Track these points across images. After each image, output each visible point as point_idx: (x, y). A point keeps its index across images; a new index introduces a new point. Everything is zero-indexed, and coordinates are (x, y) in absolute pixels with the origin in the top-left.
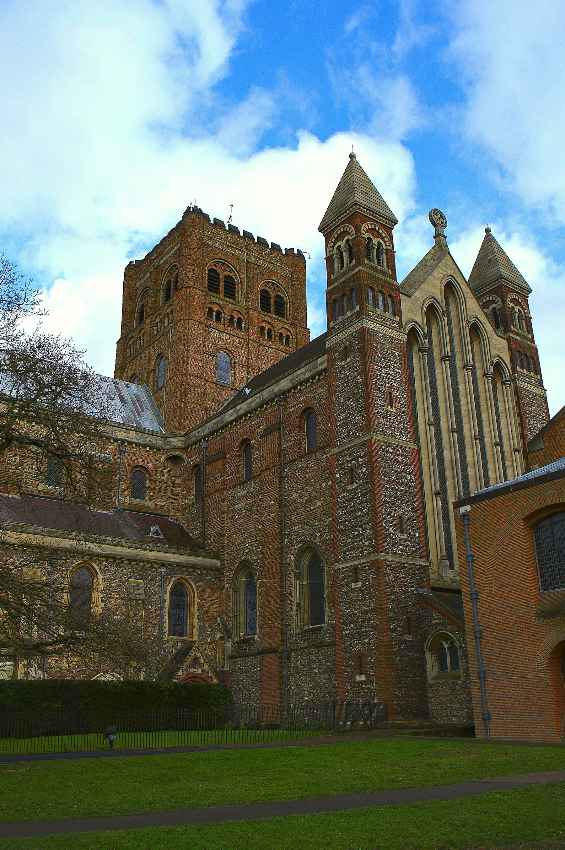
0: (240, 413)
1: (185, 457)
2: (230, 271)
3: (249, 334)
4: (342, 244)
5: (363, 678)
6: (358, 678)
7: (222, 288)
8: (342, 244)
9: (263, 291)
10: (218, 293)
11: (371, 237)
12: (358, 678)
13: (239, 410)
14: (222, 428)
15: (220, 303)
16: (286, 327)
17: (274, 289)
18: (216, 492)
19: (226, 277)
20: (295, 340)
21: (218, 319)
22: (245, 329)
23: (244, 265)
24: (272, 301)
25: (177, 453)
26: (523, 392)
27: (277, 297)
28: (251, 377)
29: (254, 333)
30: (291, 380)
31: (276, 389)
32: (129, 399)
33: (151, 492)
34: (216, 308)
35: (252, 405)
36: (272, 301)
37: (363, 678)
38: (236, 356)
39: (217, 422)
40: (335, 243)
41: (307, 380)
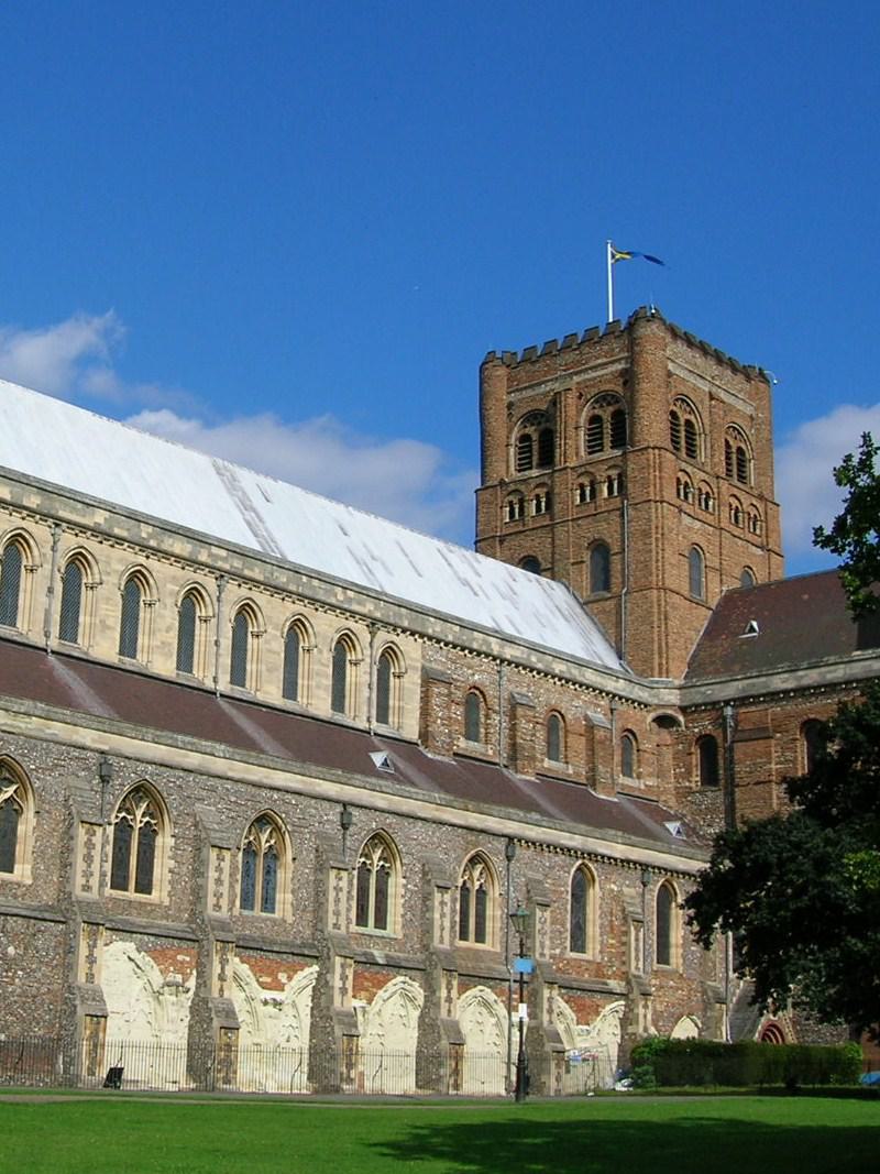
0: (805, 682)
1: (681, 718)
3: (719, 519)
13: (802, 677)
15: (689, 469)
16: (755, 503)
18: (758, 783)
22: (714, 510)
25: (670, 712)
28: (724, 588)
33: (639, 767)
38: (707, 555)
39: (754, 685)
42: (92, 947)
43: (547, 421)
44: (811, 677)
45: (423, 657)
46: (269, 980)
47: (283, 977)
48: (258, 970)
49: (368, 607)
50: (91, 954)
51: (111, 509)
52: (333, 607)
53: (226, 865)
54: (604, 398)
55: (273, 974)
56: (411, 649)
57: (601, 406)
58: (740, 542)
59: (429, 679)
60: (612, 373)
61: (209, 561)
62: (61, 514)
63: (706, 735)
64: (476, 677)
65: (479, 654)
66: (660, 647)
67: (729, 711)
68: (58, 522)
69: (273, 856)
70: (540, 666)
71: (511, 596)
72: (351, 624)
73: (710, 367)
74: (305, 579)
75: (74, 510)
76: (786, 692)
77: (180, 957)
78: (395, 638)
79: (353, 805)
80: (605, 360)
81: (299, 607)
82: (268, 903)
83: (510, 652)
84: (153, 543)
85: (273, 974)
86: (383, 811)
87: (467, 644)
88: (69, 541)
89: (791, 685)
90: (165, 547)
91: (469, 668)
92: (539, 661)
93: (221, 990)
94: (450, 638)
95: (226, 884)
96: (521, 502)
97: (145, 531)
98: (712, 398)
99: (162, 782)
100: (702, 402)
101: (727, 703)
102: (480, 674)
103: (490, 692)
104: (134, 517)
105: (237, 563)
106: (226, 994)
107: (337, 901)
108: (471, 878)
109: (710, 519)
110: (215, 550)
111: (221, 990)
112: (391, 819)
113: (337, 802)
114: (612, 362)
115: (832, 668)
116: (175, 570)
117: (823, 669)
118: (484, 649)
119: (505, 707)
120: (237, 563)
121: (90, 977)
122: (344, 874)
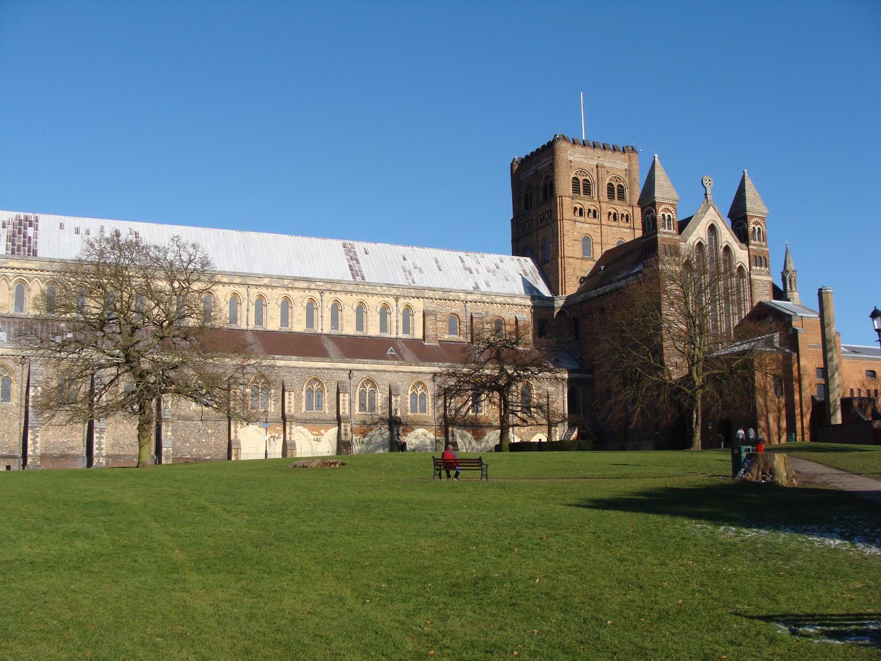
0: (600, 293)
1: (567, 312)
2: (586, 176)
4: (649, 216)
5: (658, 433)
6: (656, 433)
7: (581, 190)
9: (610, 184)
10: (580, 194)
11: (664, 213)
12: (656, 433)
14: (589, 300)
15: (582, 202)
17: (617, 181)
19: (585, 180)
20: (632, 218)
21: (581, 214)
23: (595, 169)
24: (616, 190)
26: (755, 281)
27: (620, 186)
28: (604, 251)
29: (604, 218)
32: (529, 272)
34: (578, 206)
35: (606, 290)
36: (616, 190)
37: (658, 433)
38: (593, 237)
42: (236, 428)
45: (424, 306)
46: (317, 433)
47: (323, 431)
48: (311, 430)
49: (394, 291)
50: (236, 430)
51: (271, 277)
52: (377, 294)
53: (292, 397)
55: (318, 431)
56: (418, 306)
58: (614, 228)
61: (316, 288)
62: (250, 283)
64: (453, 310)
65: (454, 300)
68: (249, 285)
69: (321, 391)
70: (488, 300)
72: (386, 299)
73: (599, 152)
74: (361, 286)
75: (255, 280)
77: (277, 428)
78: (409, 301)
79: (354, 370)
81: (360, 297)
82: (319, 406)
83: (470, 298)
84: (290, 286)
85: (318, 431)
86: (368, 371)
87: (446, 298)
88: (254, 292)
89: (595, 295)
90: (295, 286)
91: (449, 307)
92: (488, 298)
93: (290, 438)
94: (437, 297)
95: (293, 403)
97: (286, 282)
100: (592, 169)
102: (457, 308)
103: (461, 315)
104: (281, 278)
105: (329, 286)
106: (292, 439)
107: (344, 404)
108: (416, 390)
109: (595, 221)
110: (318, 283)
111: (290, 438)
112: (373, 373)
113: (347, 370)
116: (301, 293)
118: (456, 298)
119: (469, 318)
120: (329, 286)
121: (236, 437)
122: (347, 395)
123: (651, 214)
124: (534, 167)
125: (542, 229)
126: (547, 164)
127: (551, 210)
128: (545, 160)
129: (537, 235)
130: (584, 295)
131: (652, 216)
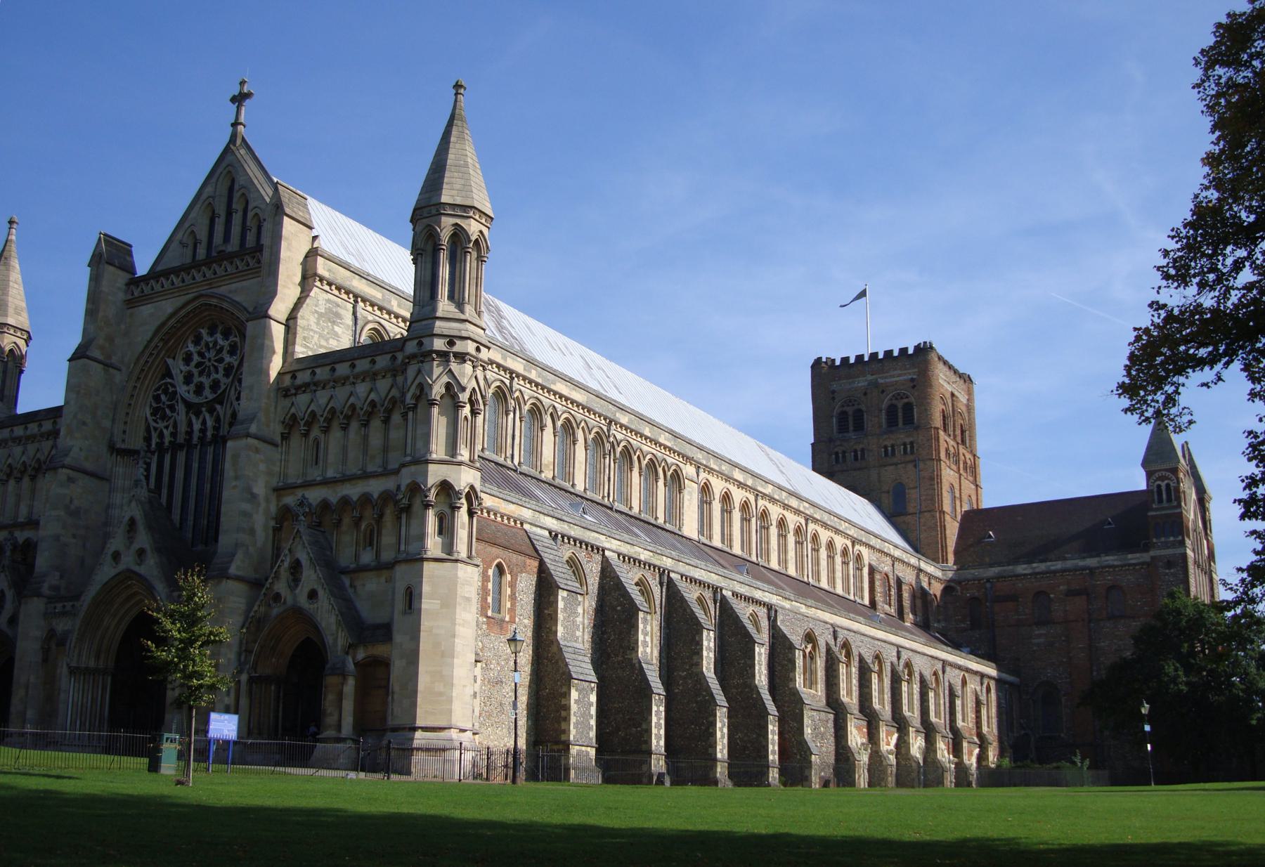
0: (1037, 570)
8: (1163, 484)
25: (952, 584)
30: (1098, 562)
31: (1081, 563)
35: (1053, 568)
39: (1005, 571)
40: (1155, 481)
41: (1117, 566)
43: (858, 404)
44: (1042, 567)
54: (899, 396)
57: (896, 399)
59: (872, 570)
60: (905, 380)
62: (760, 489)
63: (974, 598)
66: (942, 546)
67: (988, 585)
71: (869, 516)
76: (1025, 575)
80: (900, 372)
96: (844, 452)
98: (953, 395)
99: (852, 638)
101: (988, 581)
103: (891, 577)
114: (905, 374)
115: (1054, 563)
117: (1049, 564)
123: (1166, 482)
124: (870, 377)
125: (892, 468)
126: (901, 378)
127: (912, 443)
128: (900, 372)
129: (879, 474)
130: (1000, 568)
131: (1168, 486)
